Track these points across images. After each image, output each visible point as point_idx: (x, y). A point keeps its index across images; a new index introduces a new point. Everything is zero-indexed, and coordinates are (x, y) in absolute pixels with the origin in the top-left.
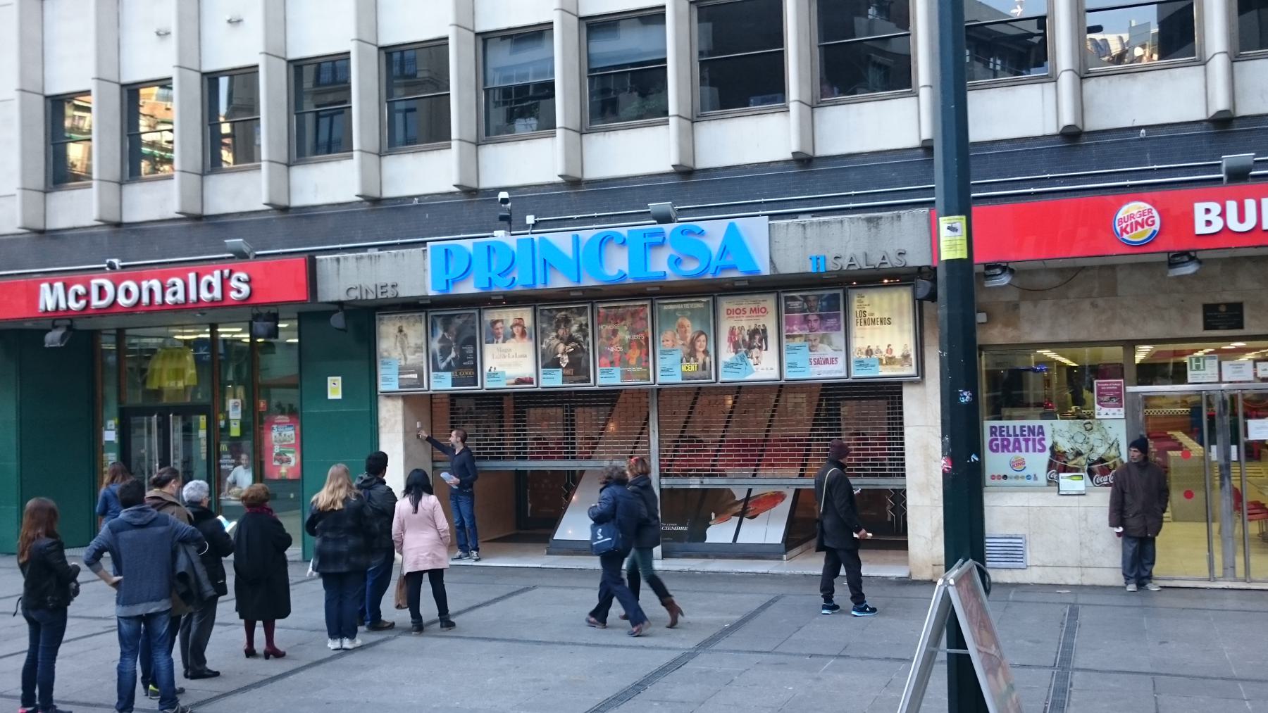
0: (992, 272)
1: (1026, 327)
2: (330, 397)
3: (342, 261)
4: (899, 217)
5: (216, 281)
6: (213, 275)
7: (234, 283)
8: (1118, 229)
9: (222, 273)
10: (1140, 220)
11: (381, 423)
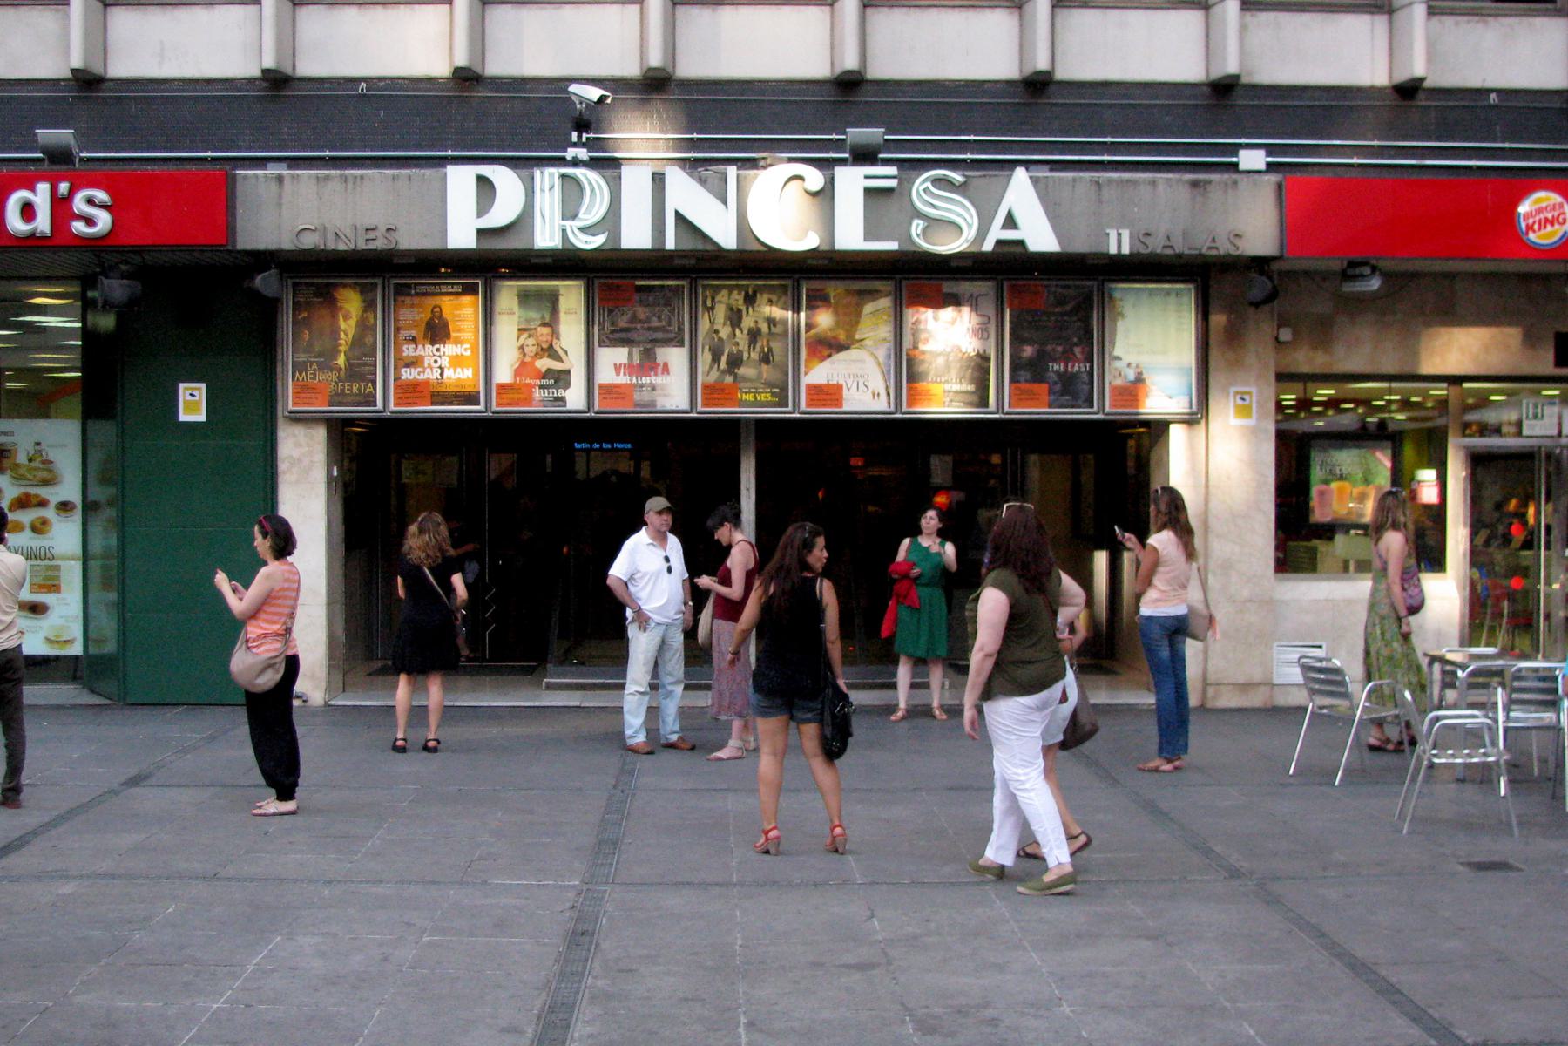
0: (1358, 271)
1: (1339, 350)
2: (184, 417)
3: (287, 182)
4: (1235, 183)
5: (41, 196)
6: (33, 189)
7: (79, 204)
8: (1523, 226)
9: (54, 190)
10: (1550, 216)
11: (283, 466)
